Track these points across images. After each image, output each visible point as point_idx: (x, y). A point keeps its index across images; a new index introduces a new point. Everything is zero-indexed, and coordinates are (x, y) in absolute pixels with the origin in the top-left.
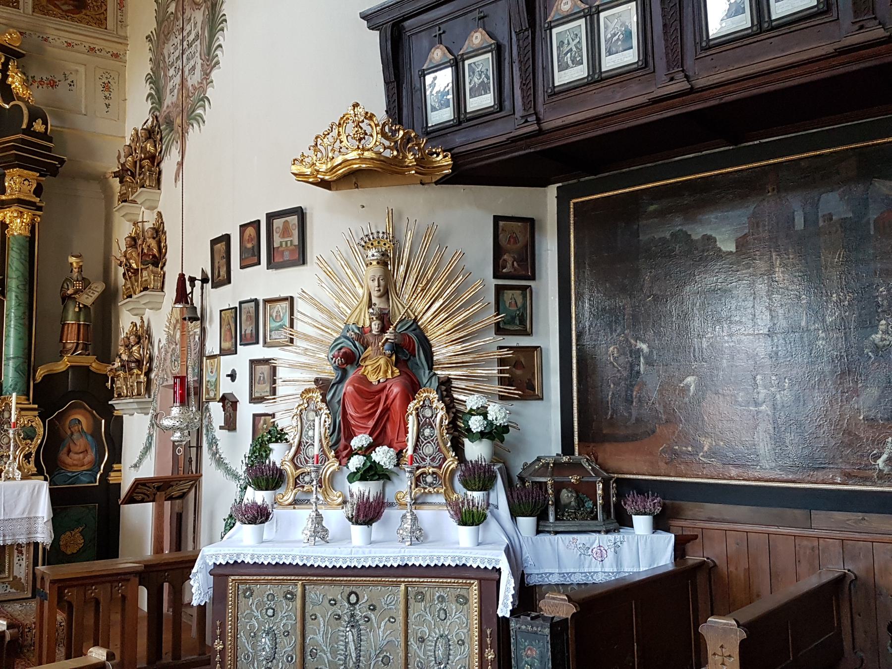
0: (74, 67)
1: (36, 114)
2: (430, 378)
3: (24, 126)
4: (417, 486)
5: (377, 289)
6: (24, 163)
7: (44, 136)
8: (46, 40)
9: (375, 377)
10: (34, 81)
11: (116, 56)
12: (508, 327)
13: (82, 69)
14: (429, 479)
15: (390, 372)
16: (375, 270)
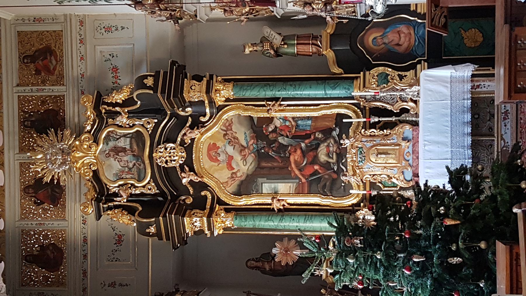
0: (98, 54)
1: (140, 83)
3: (152, 92)
6: (179, 90)
7: (156, 77)
8: (83, 75)
10: (116, 82)
11: (82, 23)
13: (99, 48)
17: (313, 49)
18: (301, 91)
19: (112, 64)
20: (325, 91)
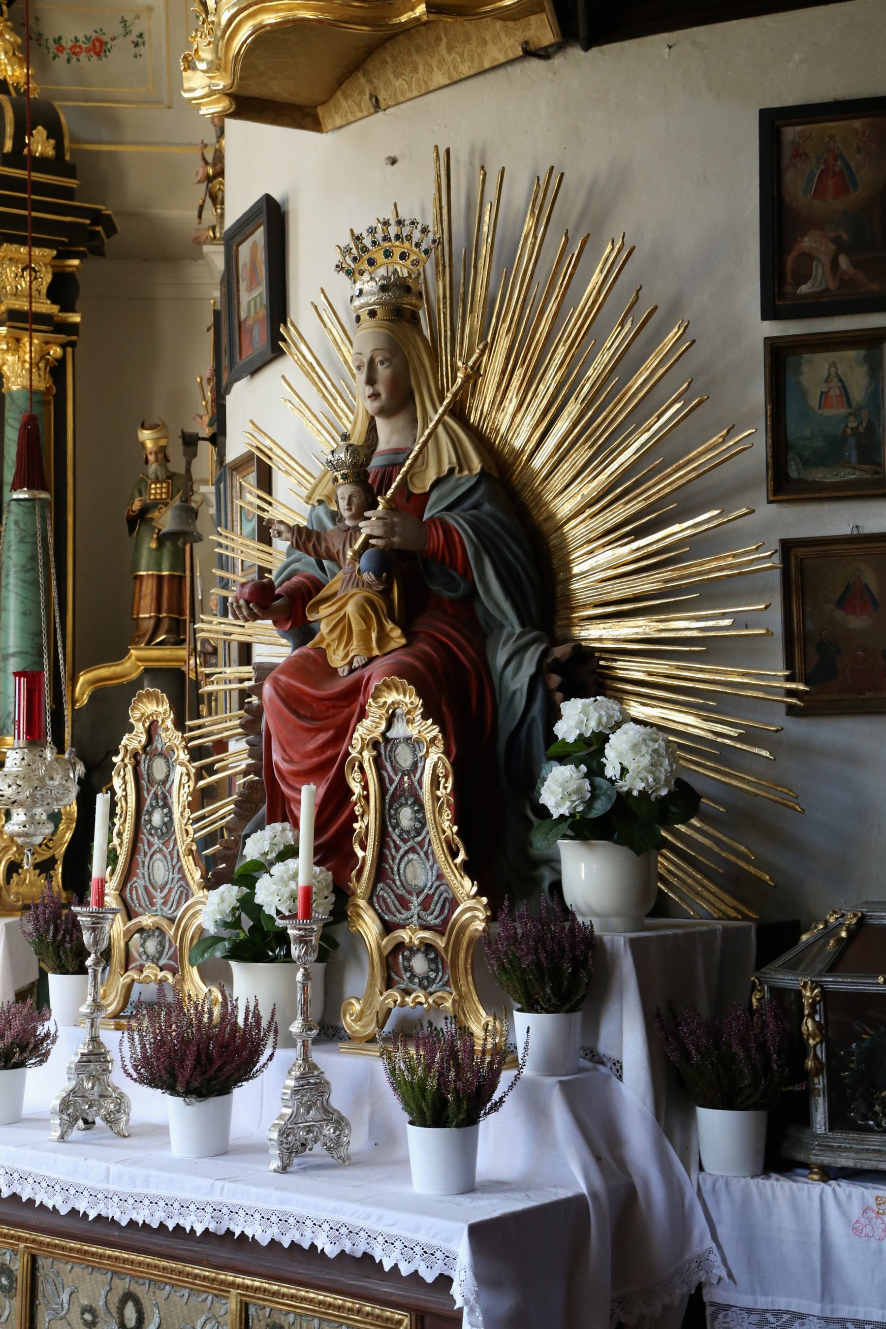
2: (518, 653)
4: (389, 984)
5: (368, 390)
9: (341, 653)
12: (820, 475)
14: (419, 964)
15: (374, 636)
16: (366, 339)
17: (147, 622)
18: (16, 586)
19: (113, 39)
20: (14, 655)
